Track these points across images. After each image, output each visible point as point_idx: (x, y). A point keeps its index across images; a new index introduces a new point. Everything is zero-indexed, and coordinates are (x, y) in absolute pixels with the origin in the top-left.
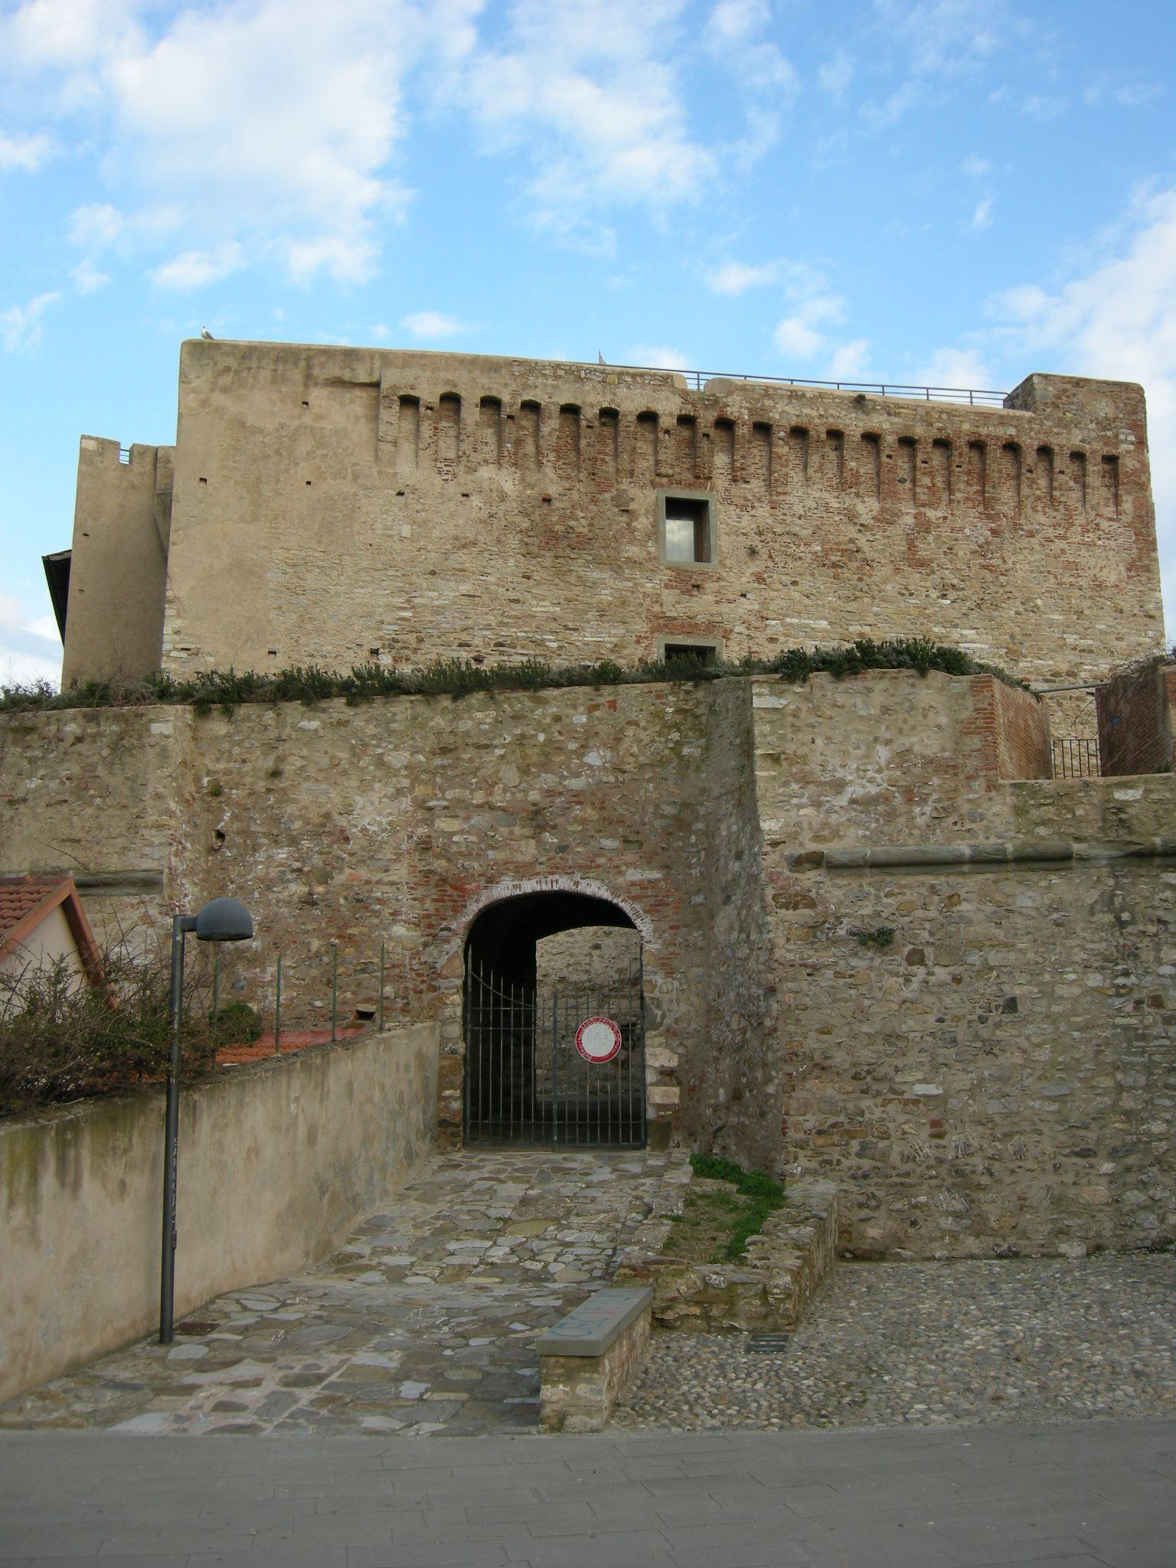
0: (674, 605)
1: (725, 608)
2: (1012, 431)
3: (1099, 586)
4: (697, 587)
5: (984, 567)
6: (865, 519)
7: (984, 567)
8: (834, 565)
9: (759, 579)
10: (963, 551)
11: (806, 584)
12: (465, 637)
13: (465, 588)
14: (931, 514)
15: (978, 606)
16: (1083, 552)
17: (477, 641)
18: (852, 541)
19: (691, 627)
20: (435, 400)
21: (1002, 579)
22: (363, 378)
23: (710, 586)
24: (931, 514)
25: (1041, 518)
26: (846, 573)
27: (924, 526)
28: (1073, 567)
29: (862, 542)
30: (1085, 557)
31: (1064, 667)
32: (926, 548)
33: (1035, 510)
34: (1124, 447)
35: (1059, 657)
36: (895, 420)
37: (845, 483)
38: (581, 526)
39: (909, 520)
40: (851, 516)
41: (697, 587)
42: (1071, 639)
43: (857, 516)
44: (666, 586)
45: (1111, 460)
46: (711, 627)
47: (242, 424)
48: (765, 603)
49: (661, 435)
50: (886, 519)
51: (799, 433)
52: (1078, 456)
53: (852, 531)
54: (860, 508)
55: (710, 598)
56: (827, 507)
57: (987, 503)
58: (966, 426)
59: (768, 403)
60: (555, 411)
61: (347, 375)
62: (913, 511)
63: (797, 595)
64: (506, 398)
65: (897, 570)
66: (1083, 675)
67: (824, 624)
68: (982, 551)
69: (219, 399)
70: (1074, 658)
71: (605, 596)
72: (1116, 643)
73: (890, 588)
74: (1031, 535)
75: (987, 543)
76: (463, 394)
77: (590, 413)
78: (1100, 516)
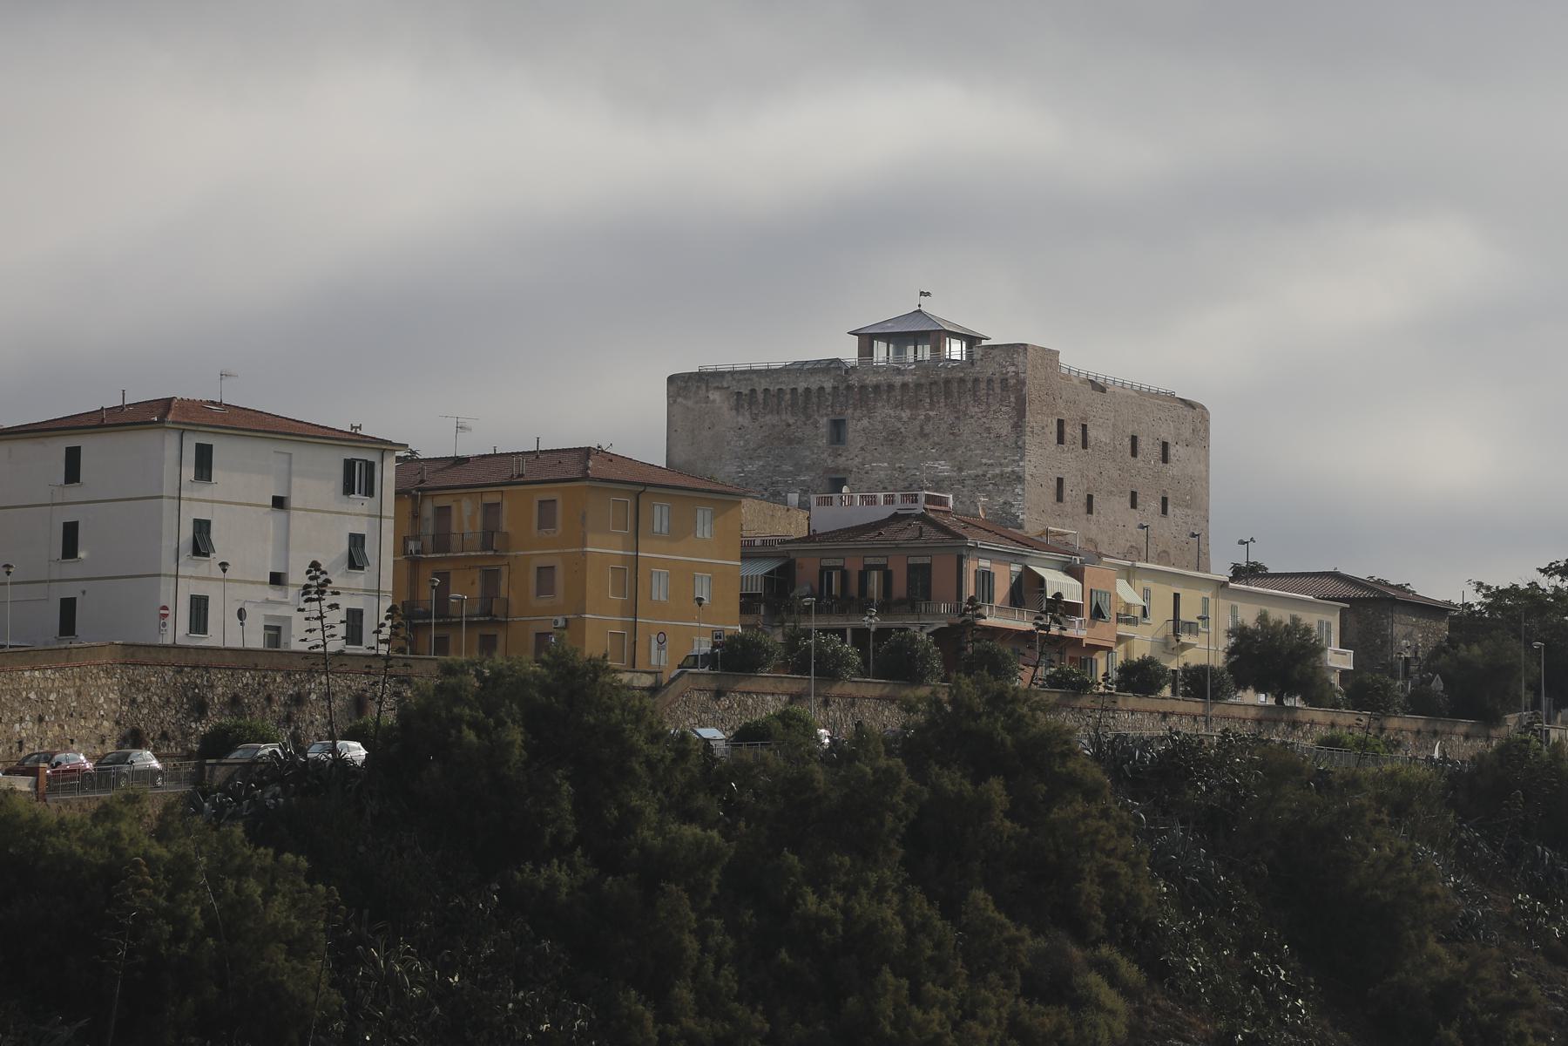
0: (830, 463)
1: (850, 462)
2: (962, 375)
3: (998, 437)
4: (839, 455)
5: (951, 434)
6: (905, 419)
7: (951, 434)
8: (891, 440)
9: (862, 449)
10: (944, 427)
11: (880, 448)
12: (761, 482)
13: (761, 463)
14: (932, 413)
15: (947, 450)
16: (993, 422)
17: (765, 483)
18: (899, 429)
19: (836, 470)
20: (747, 392)
21: (958, 438)
22: (725, 385)
23: (844, 454)
24: (931, 413)
25: (976, 409)
26: (895, 443)
27: (928, 418)
28: (988, 430)
29: (903, 430)
30: (994, 425)
31: (981, 473)
32: (927, 429)
33: (974, 406)
34: (1010, 374)
35: (978, 469)
36: (915, 377)
37: (900, 405)
38: (799, 434)
39: (923, 417)
40: (899, 419)
41: (839, 455)
42: (984, 461)
43: (902, 418)
44: (829, 456)
45: (1004, 381)
46: (845, 469)
47: (688, 408)
48: (864, 459)
49: (827, 396)
50: (913, 418)
51: (877, 388)
52: (990, 381)
53: (900, 425)
54: (903, 415)
55: (844, 459)
56: (890, 415)
57: (954, 406)
58: (943, 375)
59: (865, 377)
60: (789, 391)
61: (720, 386)
62: (924, 413)
63: (876, 454)
64: (771, 389)
65: (916, 439)
66: (988, 476)
67: (886, 464)
68: (952, 426)
69: (680, 400)
70: (984, 468)
71: (808, 462)
72: (1003, 461)
73: (911, 448)
74: (972, 417)
75: (953, 423)
76: (757, 389)
77: (800, 391)
78: (1002, 405)
